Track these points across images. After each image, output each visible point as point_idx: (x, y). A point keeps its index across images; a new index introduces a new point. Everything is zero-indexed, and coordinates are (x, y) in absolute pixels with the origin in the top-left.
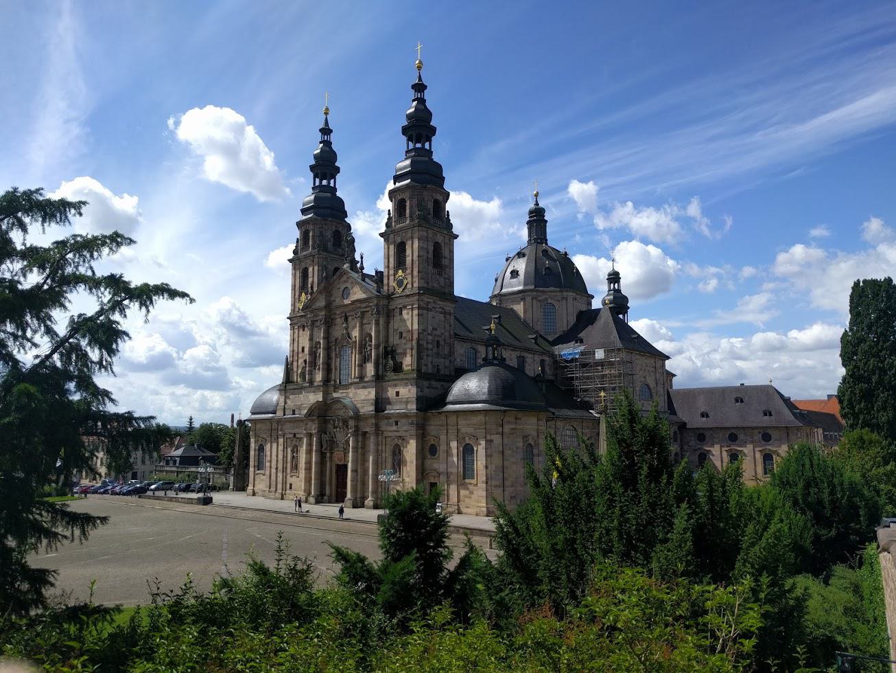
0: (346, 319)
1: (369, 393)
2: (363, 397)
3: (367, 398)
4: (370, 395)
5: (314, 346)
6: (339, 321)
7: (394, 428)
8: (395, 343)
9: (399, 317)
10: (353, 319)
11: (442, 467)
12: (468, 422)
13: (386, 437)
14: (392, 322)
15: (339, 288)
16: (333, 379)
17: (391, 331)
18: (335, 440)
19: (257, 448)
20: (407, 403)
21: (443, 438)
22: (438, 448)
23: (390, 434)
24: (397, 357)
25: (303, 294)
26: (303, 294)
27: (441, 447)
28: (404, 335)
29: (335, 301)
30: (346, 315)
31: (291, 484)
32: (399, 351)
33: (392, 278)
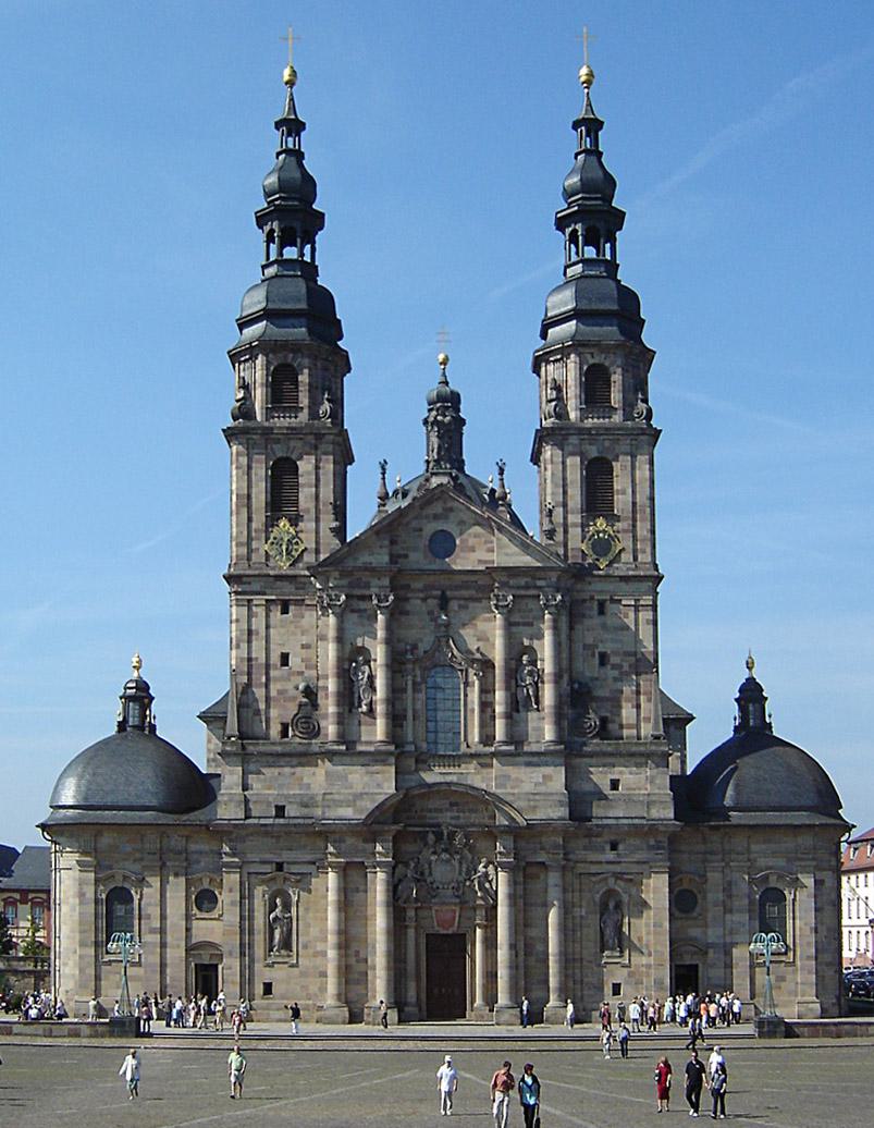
0: (444, 604)
2: (527, 787)
3: (542, 789)
4: (549, 783)
5: (347, 656)
6: (415, 604)
7: (611, 856)
8: (588, 674)
9: (597, 621)
10: (467, 607)
11: (713, 934)
12: (773, 846)
13: (581, 874)
16: (410, 739)
17: (578, 647)
18: (429, 880)
20: (649, 805)
21: (714, 877)
22: (699, 896)
23: (594, 868)
26: (283, 523)
27: (710, 896)
28: (614, 660)
30: (443, 593)
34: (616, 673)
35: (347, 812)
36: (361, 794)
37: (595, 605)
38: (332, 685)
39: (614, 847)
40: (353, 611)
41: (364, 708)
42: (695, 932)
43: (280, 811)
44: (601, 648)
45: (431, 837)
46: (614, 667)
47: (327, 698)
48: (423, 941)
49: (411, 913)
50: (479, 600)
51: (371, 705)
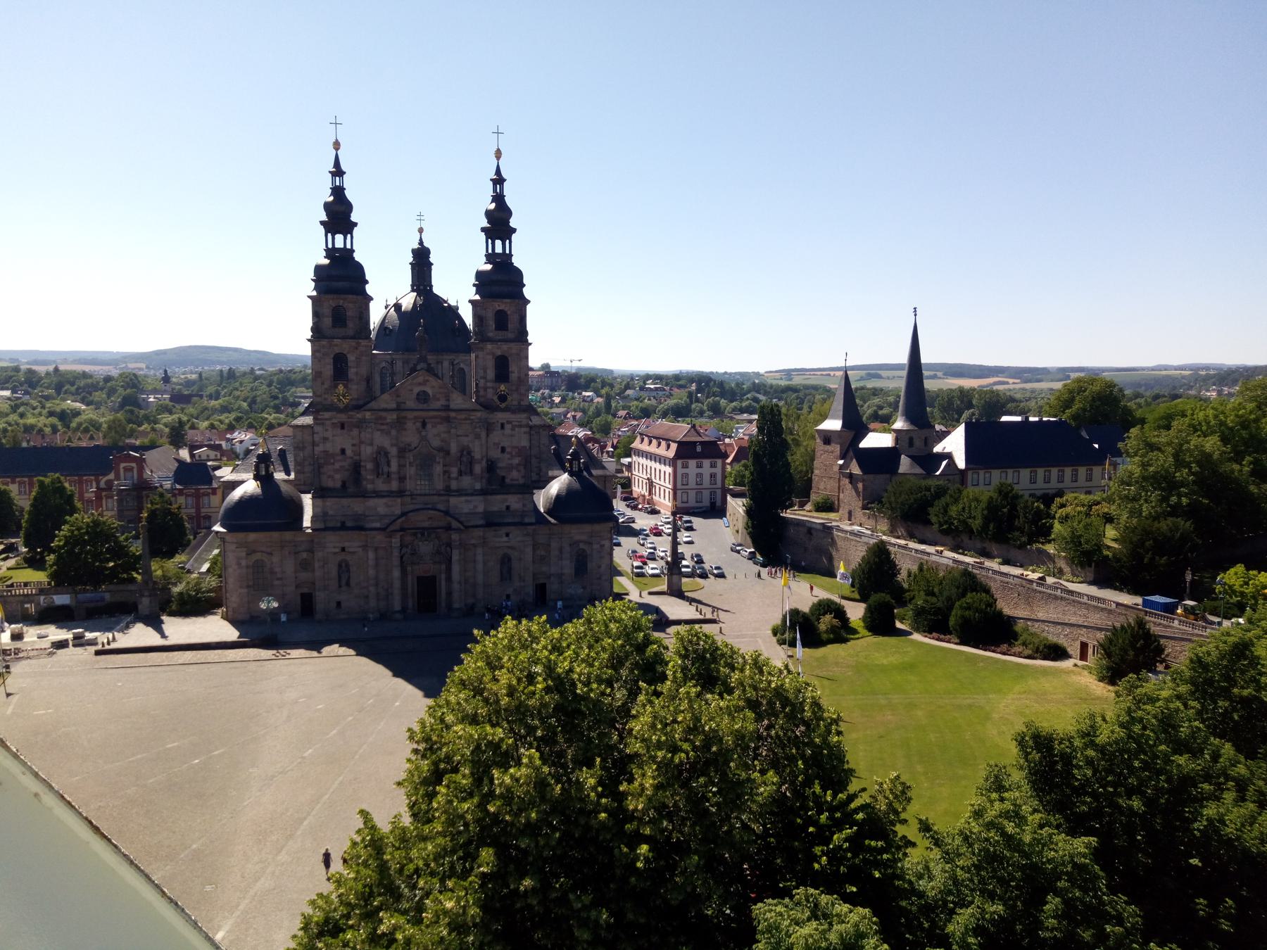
0: (424, 425)
1: (475, 507)
2: (466, 511)
6: (409, 425)
7: (505, 539)
14: (491, 435)
15: (412, 390)
16: (408, 488)
19: (251, 564)
21: (554, 545)
24: (498, 471)
25: (341, 387)
26: (341, 387)
28: (508, 450)
29: (405, 403)
31: (339, 604)
32: (500, 465)
33: (490, 391)
34: (509, 456)
35: (378, 525)
36: (386, 516)
37: (499, 425)
38: (370, 466)
39: (507, 535)
40: (378, 430)
41: (385, 476)
42: (544, 569)
43: (343, 523)
44: (502, 445)
45: (419, 535)
46: (508, 453)
47: (366, 470)
48: (415, 580)
49: (409, 568)
50: (441, 423)
51: (389, 475)
